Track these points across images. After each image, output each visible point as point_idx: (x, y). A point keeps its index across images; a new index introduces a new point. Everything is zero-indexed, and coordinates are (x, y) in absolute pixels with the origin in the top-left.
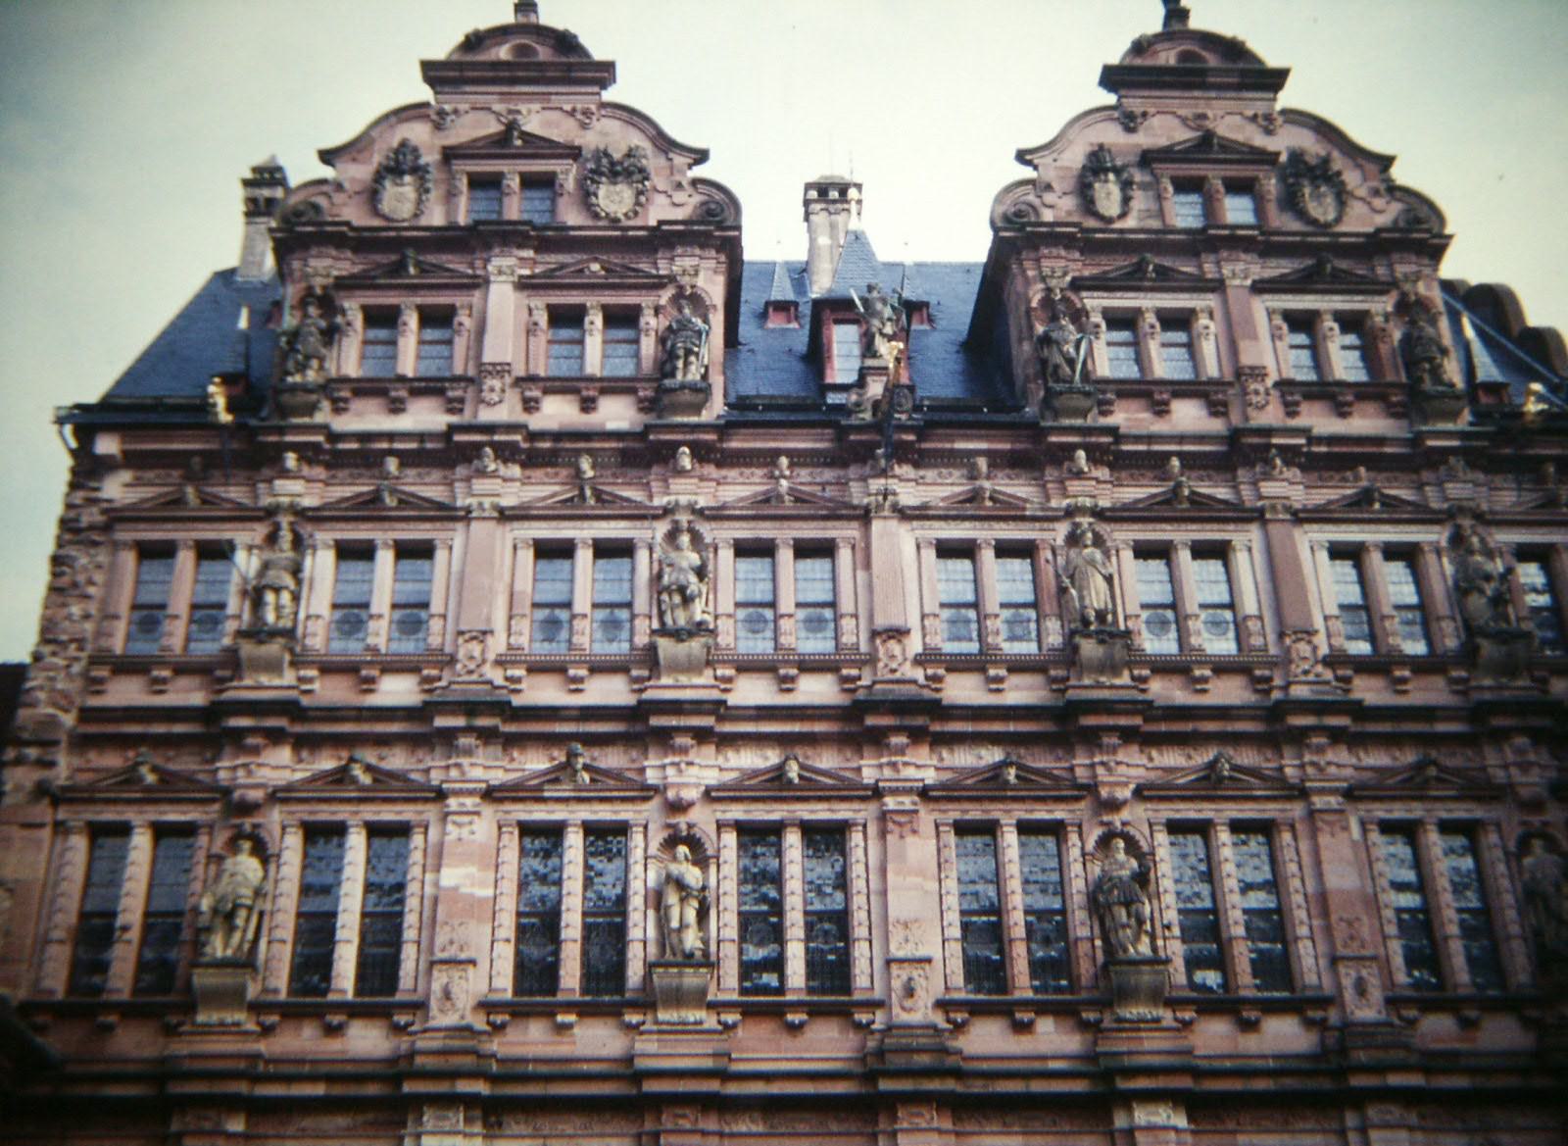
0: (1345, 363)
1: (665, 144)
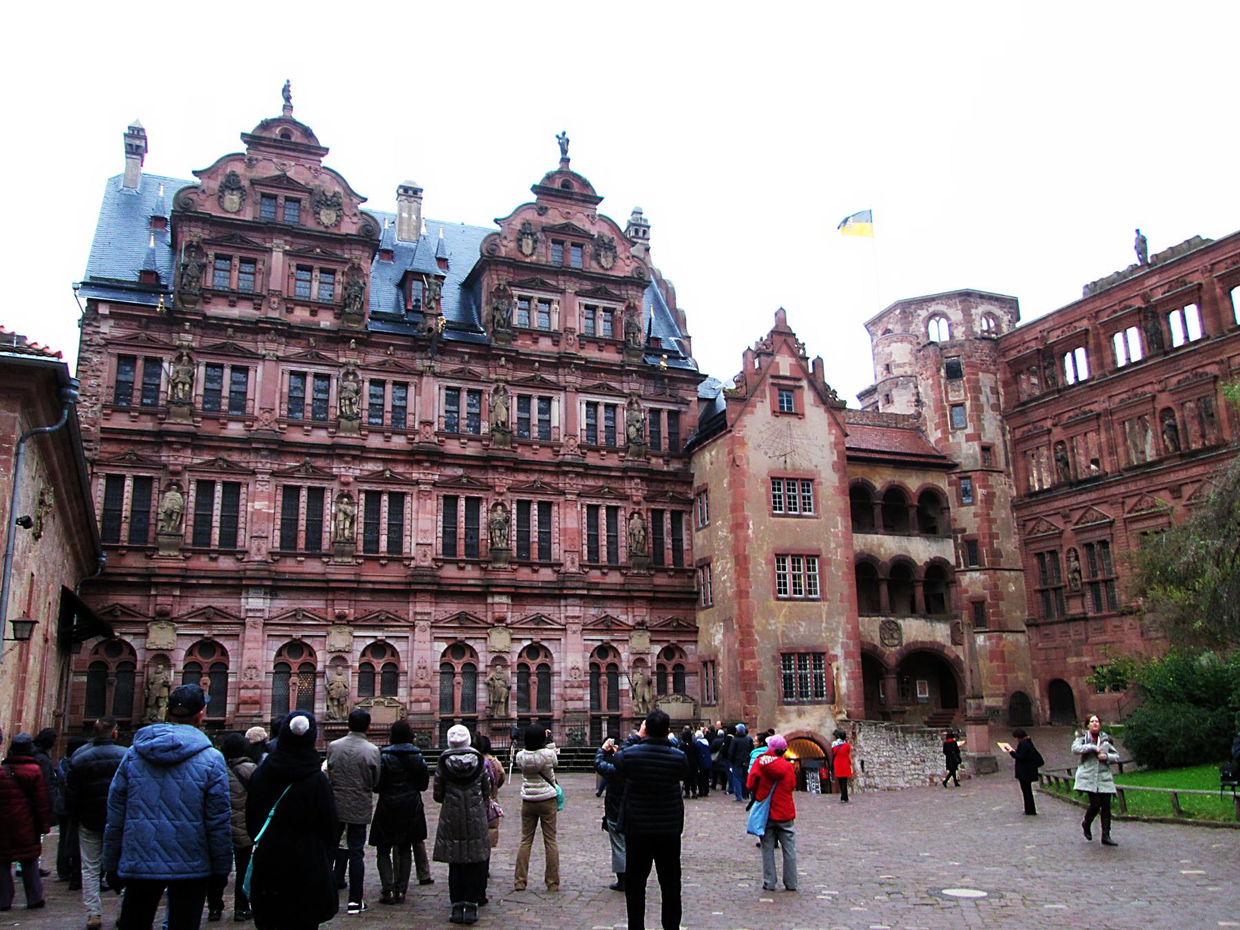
0: (602, 329)
1: (350, 193)
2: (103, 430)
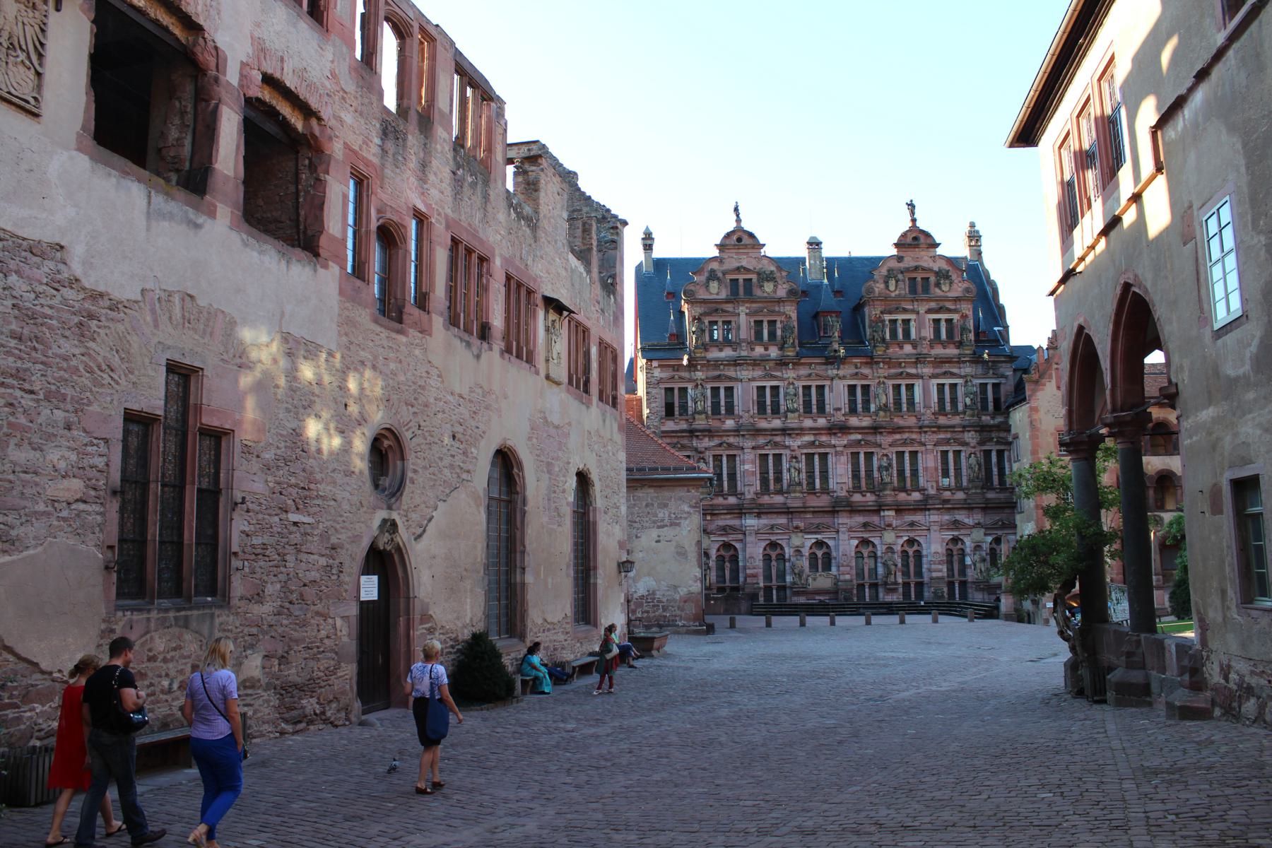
2: (663, 432)
